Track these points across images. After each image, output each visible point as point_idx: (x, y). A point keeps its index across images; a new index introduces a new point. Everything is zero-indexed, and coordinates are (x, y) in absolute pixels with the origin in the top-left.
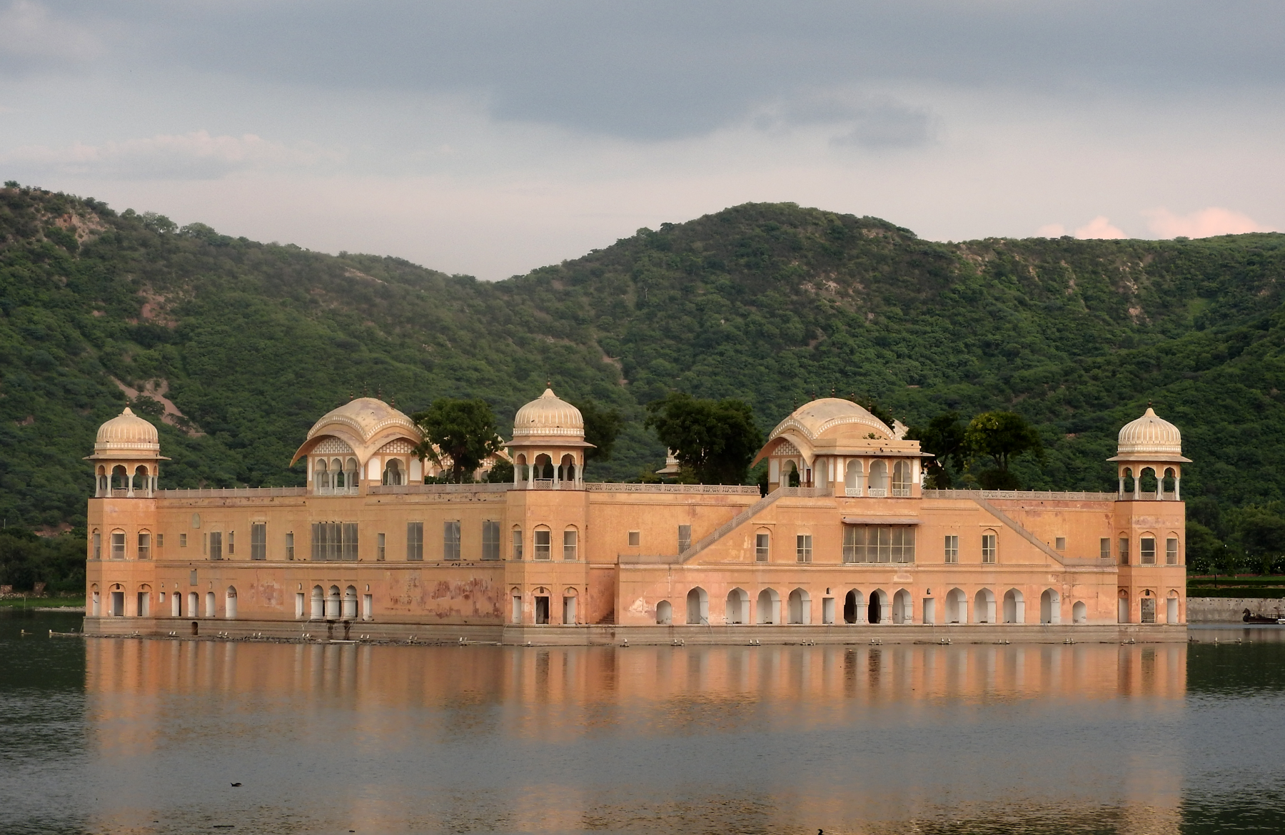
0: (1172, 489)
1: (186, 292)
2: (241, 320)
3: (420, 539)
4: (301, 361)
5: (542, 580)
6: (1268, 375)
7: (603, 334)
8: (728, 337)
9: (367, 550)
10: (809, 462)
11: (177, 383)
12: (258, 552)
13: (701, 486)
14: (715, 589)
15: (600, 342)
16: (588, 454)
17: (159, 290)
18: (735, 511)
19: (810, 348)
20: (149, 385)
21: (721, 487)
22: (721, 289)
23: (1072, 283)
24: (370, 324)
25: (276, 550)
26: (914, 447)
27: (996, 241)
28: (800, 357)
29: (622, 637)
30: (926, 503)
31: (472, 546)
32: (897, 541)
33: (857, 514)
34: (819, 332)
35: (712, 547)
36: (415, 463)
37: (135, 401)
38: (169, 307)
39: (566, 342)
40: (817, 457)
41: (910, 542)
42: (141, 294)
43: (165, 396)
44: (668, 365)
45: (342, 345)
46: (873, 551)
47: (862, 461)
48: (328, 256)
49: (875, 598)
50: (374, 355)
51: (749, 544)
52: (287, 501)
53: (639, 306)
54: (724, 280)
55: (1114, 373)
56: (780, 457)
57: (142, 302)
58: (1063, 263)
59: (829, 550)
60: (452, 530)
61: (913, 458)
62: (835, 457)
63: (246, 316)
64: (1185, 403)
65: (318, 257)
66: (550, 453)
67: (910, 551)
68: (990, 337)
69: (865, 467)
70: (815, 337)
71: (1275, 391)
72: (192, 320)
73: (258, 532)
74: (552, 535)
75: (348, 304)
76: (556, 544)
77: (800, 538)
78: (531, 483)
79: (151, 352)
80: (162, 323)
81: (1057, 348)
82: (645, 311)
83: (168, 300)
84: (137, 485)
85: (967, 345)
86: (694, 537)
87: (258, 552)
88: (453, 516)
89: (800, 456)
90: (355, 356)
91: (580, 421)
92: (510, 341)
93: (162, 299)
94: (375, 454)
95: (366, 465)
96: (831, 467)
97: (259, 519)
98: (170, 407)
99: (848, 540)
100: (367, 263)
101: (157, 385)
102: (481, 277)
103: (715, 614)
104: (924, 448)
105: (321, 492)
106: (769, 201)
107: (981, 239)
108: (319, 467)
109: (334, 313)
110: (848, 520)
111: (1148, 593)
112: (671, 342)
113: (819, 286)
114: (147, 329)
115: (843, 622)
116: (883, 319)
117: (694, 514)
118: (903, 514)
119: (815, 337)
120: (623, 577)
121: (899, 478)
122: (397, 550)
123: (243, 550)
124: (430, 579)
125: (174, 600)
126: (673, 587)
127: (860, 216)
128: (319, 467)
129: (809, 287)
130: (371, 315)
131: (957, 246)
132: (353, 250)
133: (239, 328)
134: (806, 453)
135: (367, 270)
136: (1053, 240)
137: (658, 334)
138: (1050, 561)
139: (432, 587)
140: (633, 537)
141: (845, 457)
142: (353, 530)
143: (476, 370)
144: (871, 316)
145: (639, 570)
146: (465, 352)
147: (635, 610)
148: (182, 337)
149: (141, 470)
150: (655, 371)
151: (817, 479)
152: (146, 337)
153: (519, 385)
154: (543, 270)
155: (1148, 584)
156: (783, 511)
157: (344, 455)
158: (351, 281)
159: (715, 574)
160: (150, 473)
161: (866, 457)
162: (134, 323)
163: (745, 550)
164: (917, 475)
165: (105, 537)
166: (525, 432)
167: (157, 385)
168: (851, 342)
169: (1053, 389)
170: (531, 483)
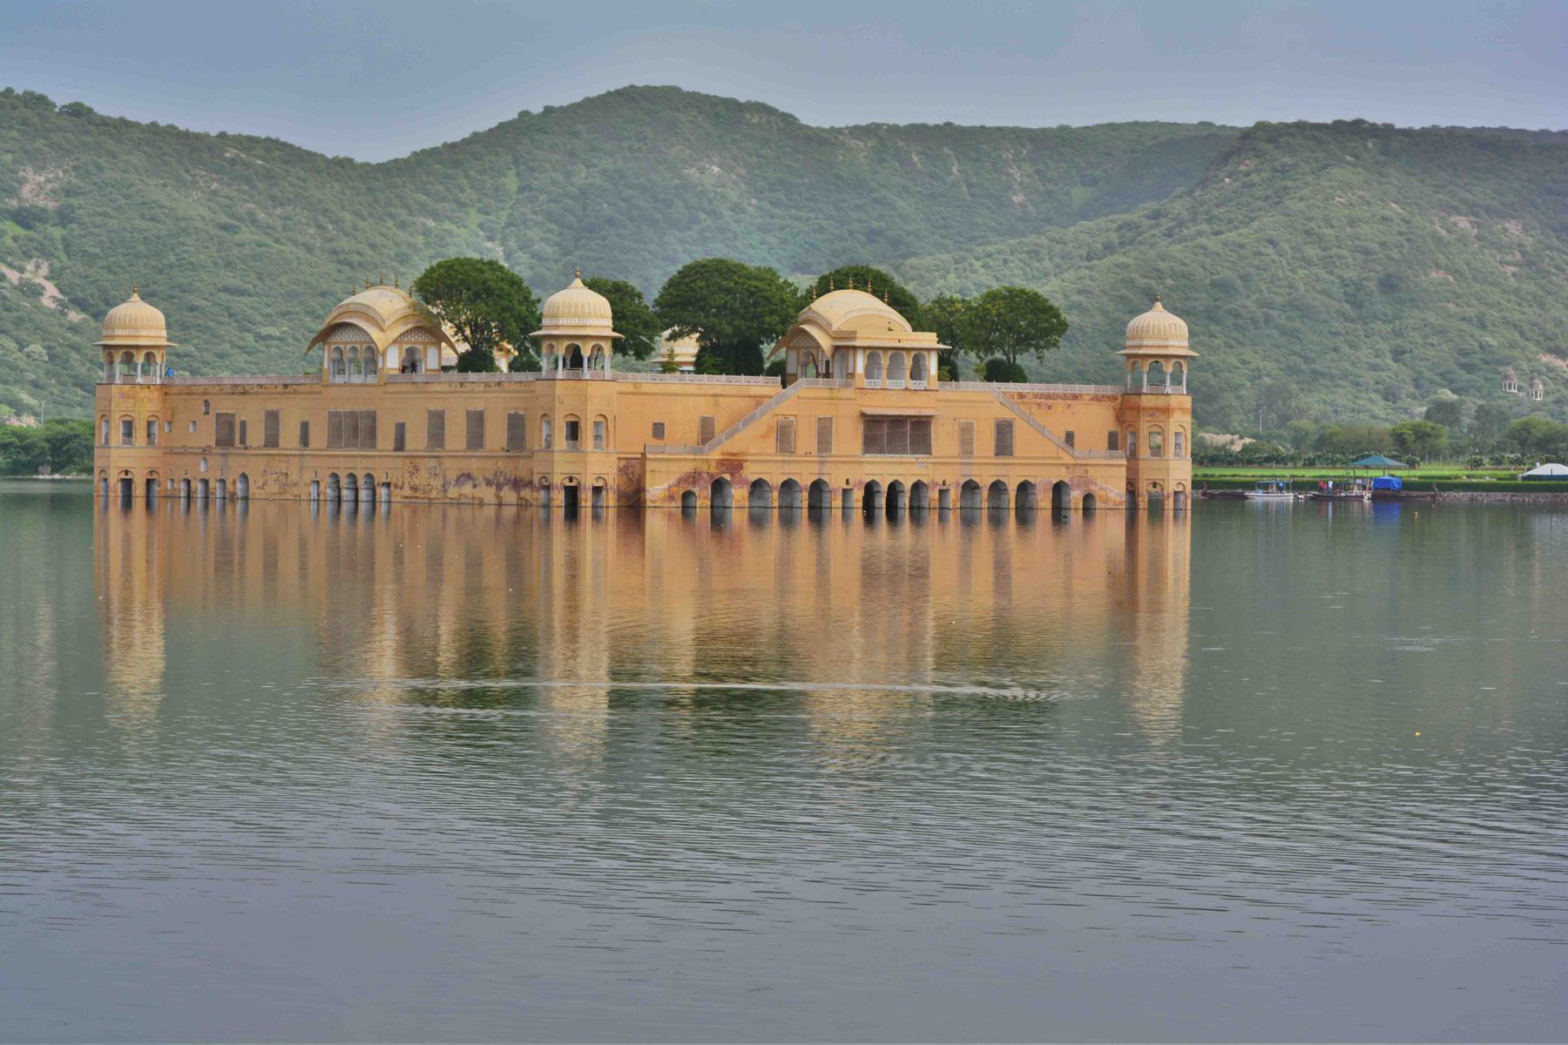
0: (1180, 383)
1: (65, 172)
2: (122, 201)
3: (442, 426)
4: (183, 244)
5: (570, 469)
6: (1163, 265)
7: (482, 218)
8: (610, 221)
9: (386, 440)
10: (829, 355)
11: (57, 264)
12: (272, 441)
13: (724, 377)
15: (481, 226)
16: (618, 347)
17: (39, 169)
18: (753, 402)
19: (694, 233)
20: (30, 267)
21: (743, 378)
22: (604, 173)
23: (954, 169)
24: (252, 205)
25: (289, 436)
26: (929, 339)
27: (878, 126)
28: (683, 242)
30: (941, 395)
31: (496, 435)
34: (703, 216)
35: (737, 436)
36: (432, 352)
37: (16, 282)
38: (49, 186)
39: (447, 225)
40: (837, 348)
42: (21, 174)
43: (46, 278)
44: (549, 250)
45: (224, 227)
48: (207, 135)
49: (894, 489)
50: (256, 237)
52: (301, 389)
53: (521, 190)
54: (607, 163)
55: (1005, 262)
56: (798, 349)
57: (26, 180)
58: (946, 150)
59: (848, 438)
60: (477, 421)
61: (929, 350)
62: (855, 348)
63: (126, 197)
64: (1080, 292)
65: (197, 137)
66: (579, 343)
68: (875, 224)
69: (885, 361)
70: (697, 222)
71: (1169, 281)
72: (72, 201)
73: (273, 418)
74: (582, 425)
75: (229, 185)
76: (587, 432)
78: (561, 373)
79: (31, 233)
80: (41, 203)
81: (942, 236)
82: (526, 194)
83: (48, 181)
84: (145, 373)
85: (851, 233)
86: (717, 429)
87: (272, 441)
88: (478, 405)
89: (818, 346)
90: (237, 238)
91: (609, 313)
92: (390, 224)
93: (42, 179)
94: (395, 342)
95: (384, 354)
96: (851, 359)
97: (272, 406)
98: (51, 289)
100: (249, 143)
101: (38, 266)
102: (359, 158)
104: (941, 340)
105: (339, 379)
106: (652, 84)
107: (863, 123)
108: (335, 355)
109: (215, 193)
110: (868, 411)
111: (1155, 485)
112: (554, 227)
113: (702, 170)
114: (26, 210)
116: (768, 206)
117: (716, 404)
119: (697, 222)
120: (649, 466)
121: (917, 373)
122: (417, 439)
123: (256, 436)
124: (452, 469)
125: (183, 486)
127: (742, 100)
128: (335, 355)
129: (693, 171)
130: (251, 196)
131: (839, 131)
132: (230, 132)
133: (119, 209)
134: (826, 343)
135: (248, 150)
136: (937, 127)
137: (539, 218)
138: (1062, 454)
139: (452, 476)
140: (658, 430)
141: (864, 348)
142: (373, 417)
143: (359, 253)
144: (754, 201)
146: (346, 234)
148: (64, 218)
149: (149, 356)
150: (534, 255)
151: (835, 368)
152: (25, 218)
153: (402, 269)
154: (423, 151)
155: (1156, 476)
156: (804, 399)
157: (361, 343)
158: (233, 162)
160: (159, 360)
161: (885, 349)
162: (15, 203)
165: (113, 424)
166: (553, 322)
167: (38, 266)
168: (734, 226)
169: (944, 277)
170: (561, 373)
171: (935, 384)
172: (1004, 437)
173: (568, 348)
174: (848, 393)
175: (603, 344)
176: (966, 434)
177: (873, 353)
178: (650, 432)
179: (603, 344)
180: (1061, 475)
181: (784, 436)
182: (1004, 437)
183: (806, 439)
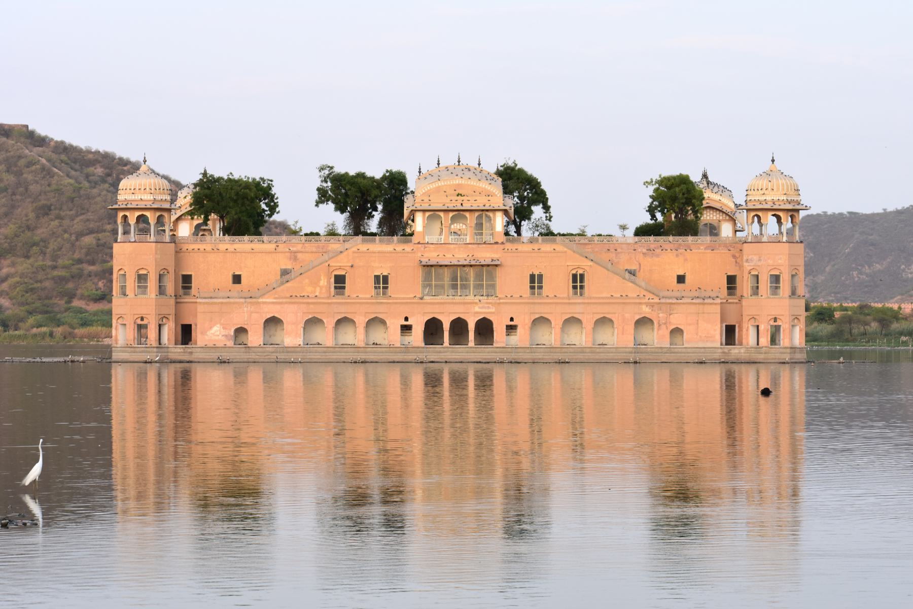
14: (293, 317)
29: (198, 355)
32: (479, 277)
33: (432, 256)
35: (288, 285)
41: (491, 277)
46: (454, 287)
47: (442, 214)
49: (459, 327)
51: (326, 282)
67: (493, 286)
77: (377, 278)
99: (427, 278)
103: (291, 337)
115: (423, 344)
117: (295, 259)
118: (485, 255)
126: (252, 318)
140: (237, 279)
141: (424, 211)
145: (215, 303)
147: (212, 333)
159: (292, 306)
161: (446, 211)
163: (321, 288)
164: (499, 222)
171: (503, 238)
172: (578, 281)
173: (139, 218)
174: (408, 248)
175: (147, 214)
176: (536, 281)
177: (433, 214)
178: (231, 279)
179: (147, 214)
180: (646, 311)
181: (340, 281)
182: (578, 281)
183: (360, 286)
